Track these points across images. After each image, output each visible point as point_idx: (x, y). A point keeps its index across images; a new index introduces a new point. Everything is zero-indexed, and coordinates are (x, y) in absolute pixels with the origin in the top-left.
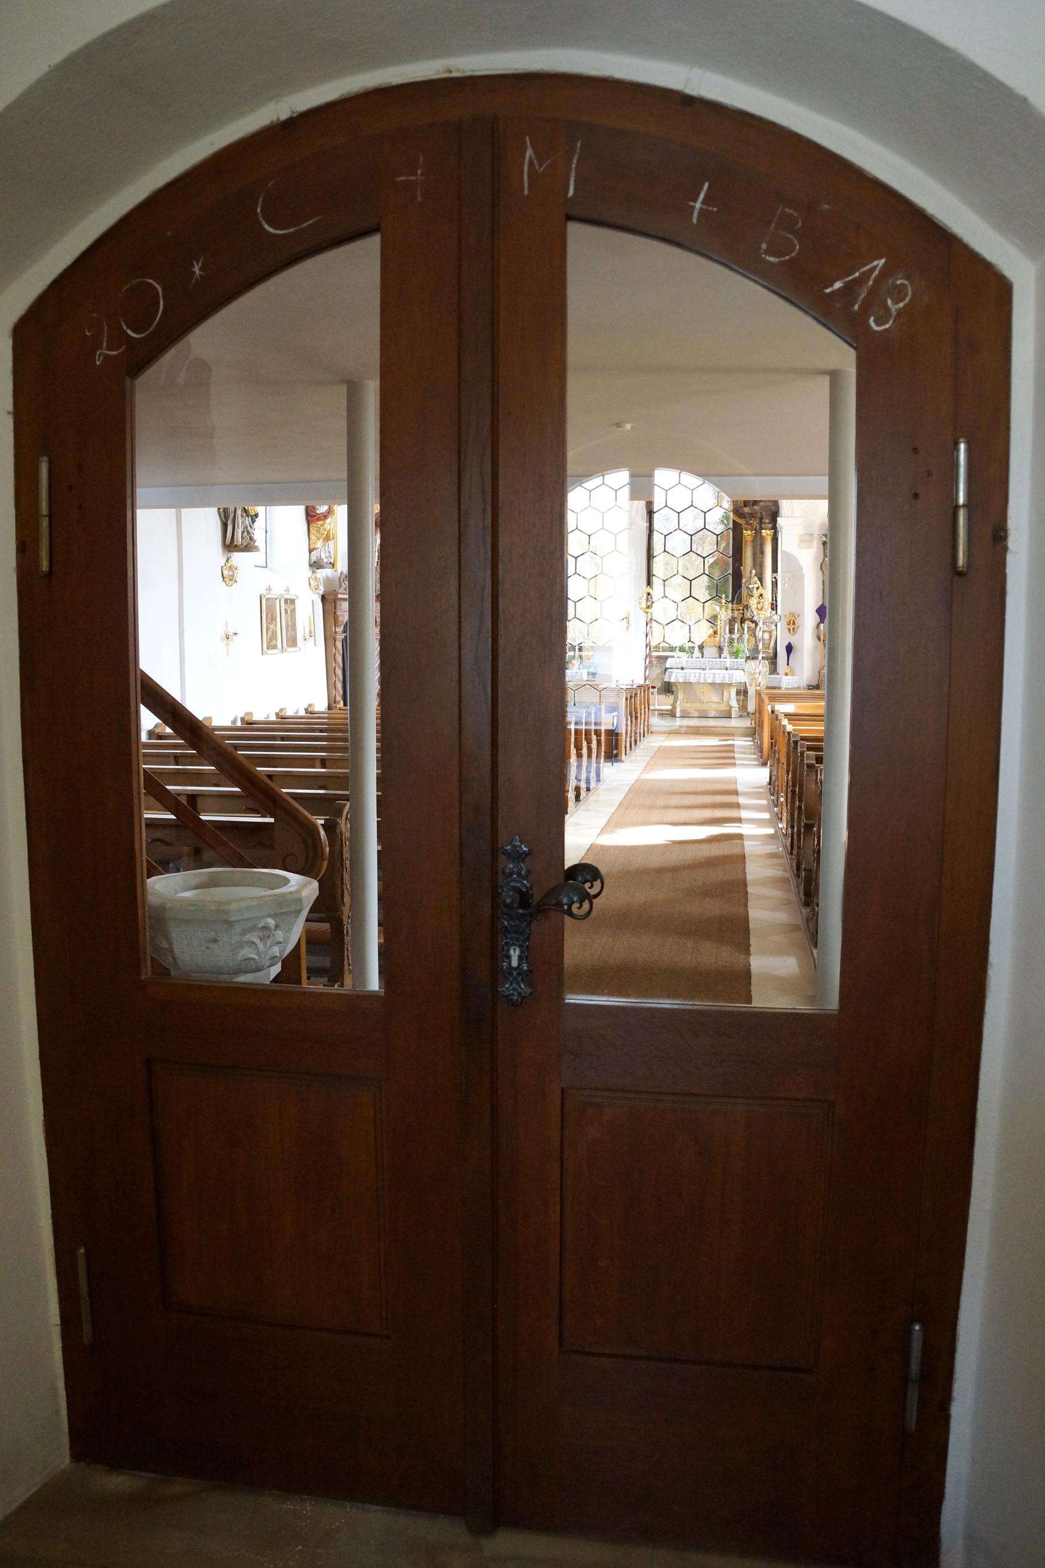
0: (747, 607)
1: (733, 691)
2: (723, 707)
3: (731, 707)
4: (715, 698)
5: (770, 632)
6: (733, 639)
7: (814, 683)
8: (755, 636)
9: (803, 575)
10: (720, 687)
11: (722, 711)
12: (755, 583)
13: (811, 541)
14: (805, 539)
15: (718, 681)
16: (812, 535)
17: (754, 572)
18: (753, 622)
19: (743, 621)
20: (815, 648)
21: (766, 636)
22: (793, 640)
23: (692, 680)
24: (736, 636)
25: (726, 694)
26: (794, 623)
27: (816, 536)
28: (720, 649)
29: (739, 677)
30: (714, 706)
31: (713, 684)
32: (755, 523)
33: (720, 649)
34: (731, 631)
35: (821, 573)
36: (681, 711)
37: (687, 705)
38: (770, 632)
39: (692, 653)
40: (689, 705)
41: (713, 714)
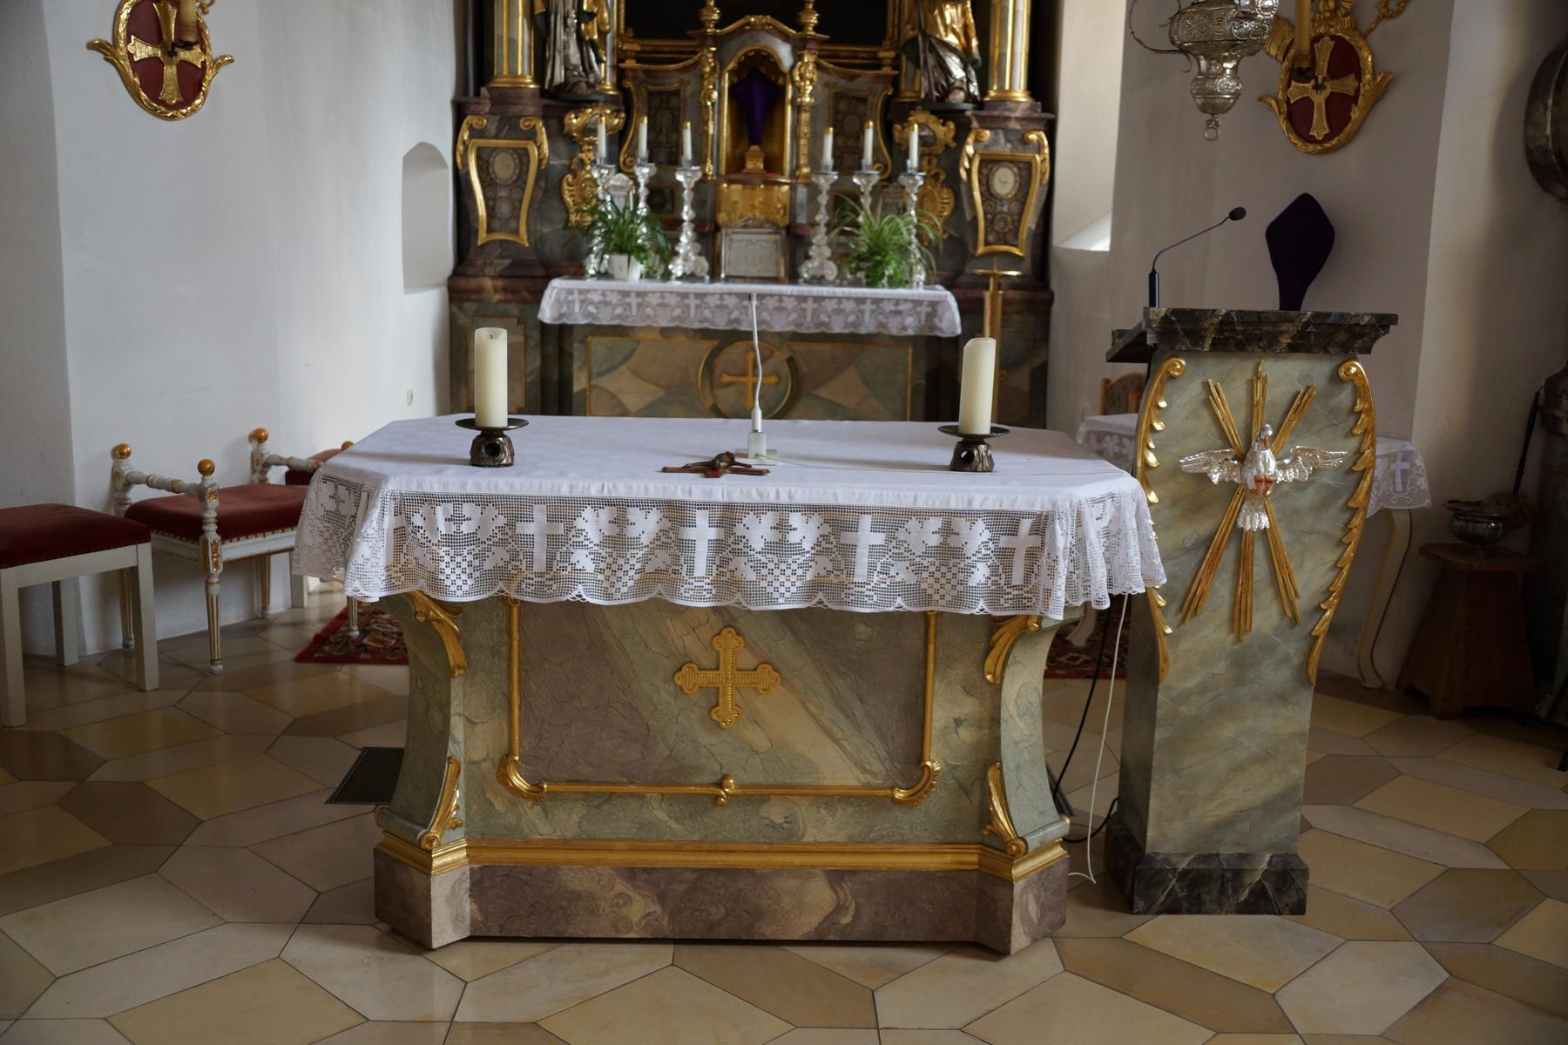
1: (1024, 679)
2: (920, 851)
3: (999, 850)
4: (839, 759)
5: (1025, 171)
6: (855, 195)
10: (882, 657)
11: (903, 886)
15: (877, 585)
18: (945, 112)
19: (893, 117)
21: (1005, 181)
22: (1337, 178)
23: (587, 578)
25: (948, 711)
26: (1345, 61)
28: (794, 242)
30: (822, 827)
31: (822, 629)
33: (794, 242)
34: (848, 158)
36: (482, 882)
37: (539, 824)
38: (1025, 171)
39: (669, 255)
40: (569, 820)
41: (815, 903)
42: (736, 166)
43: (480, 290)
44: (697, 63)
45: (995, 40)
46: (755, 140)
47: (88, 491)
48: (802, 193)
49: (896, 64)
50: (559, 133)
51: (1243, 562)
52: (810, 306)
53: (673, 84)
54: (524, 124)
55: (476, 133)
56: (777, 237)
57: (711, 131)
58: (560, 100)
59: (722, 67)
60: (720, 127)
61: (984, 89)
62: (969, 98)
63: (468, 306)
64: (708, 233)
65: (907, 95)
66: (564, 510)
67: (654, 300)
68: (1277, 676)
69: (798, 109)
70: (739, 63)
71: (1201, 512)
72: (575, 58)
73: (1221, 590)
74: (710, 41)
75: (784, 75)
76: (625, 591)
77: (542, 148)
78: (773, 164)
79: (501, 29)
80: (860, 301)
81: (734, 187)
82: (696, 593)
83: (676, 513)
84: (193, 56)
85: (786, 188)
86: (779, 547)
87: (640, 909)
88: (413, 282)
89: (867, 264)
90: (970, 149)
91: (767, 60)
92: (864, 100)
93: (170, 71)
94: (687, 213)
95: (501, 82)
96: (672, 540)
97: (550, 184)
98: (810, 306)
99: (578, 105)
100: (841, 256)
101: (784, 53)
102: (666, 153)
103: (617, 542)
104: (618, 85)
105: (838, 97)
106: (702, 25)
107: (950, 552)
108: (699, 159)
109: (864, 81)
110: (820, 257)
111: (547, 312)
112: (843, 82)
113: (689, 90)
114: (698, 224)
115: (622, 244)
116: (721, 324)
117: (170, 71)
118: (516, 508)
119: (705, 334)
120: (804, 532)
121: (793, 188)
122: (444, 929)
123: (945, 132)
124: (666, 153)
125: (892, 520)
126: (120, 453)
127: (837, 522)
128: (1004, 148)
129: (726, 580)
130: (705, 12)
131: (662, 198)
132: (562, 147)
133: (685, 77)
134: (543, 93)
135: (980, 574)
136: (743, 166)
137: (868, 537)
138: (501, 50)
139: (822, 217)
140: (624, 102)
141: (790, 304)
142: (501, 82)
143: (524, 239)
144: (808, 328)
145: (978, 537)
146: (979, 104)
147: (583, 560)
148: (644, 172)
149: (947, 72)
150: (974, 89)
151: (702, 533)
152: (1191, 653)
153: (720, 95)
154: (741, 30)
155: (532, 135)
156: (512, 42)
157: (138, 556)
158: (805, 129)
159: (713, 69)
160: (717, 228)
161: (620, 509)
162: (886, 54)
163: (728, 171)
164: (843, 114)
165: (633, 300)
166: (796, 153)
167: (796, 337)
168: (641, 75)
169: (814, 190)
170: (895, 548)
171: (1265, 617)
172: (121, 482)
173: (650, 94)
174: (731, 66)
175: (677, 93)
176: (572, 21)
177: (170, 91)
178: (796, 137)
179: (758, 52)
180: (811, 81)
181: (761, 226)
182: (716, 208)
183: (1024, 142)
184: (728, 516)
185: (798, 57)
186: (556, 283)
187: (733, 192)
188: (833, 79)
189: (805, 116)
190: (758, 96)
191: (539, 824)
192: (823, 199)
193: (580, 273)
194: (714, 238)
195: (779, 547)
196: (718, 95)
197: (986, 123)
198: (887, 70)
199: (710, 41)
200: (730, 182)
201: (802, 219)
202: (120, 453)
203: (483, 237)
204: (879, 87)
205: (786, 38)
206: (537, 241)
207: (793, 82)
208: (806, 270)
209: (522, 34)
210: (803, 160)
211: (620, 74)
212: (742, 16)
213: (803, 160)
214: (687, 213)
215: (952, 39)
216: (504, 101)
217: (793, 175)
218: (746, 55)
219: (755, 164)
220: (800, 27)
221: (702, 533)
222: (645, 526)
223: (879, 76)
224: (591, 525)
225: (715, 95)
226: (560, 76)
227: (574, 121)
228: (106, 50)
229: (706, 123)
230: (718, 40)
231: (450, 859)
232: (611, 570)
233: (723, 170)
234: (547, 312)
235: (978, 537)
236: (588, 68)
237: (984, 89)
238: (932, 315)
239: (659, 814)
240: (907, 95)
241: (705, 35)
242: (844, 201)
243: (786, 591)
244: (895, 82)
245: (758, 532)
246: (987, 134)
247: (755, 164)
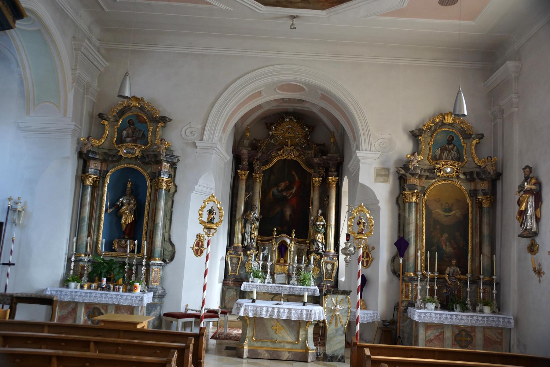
0: (314, 241)
1: (311, 330)
2: (298, 348)
3: (307, 349)
4: (290, 338)
5: (333, 265)
6: (301, 268)
7: (389, 318)
8: (319, 267)
9: (379, 208)
10: (295, 326)
11: (296, 354)
12: (321, 223)
13: (388, 176)
14: (382, 174)
15: (294, 317)
16: (388, 170)
17: (320, 211)
18: (318, 254)
19: (309, 253)
20: (390, 282)
21: (329, 267)
22: (368, 272)
23: (264, 315)
24: (303, 265)
25: (302, 333)
26: (368, 256)
27: (392, 170)
28: (289, 277)
29: (318, 312)
30: (288, 346)
31: (288, 322)
32: (322, 171)
33: (289, 277)
35: (396, 207)
36: (249, 351)
37: (256, 344)
38: (333, 265)
39: (265, 278)
40: (259, 344)
41: (286, 355)
42: (278, 262)
43: (229, 284)
45: (328, 240)
47: (182, 310)
48: (291, 267)
49: (309, 244)
50: (245, 254)
51: (336, 319)
52: (291, 289)
54: (239, 253)
55: (230, 254)
58: (246, 249)
60: (276, 254)
61: (326, 249)
62: (323, 251)
63: (226, 287)
64: (273, 274)
65: (312, 249)
66: (262, 307)
67: (262, 287)
68: (341, 332)
69: (291, 252)
71: (331, 311)
72: (249, 241)
73: (334, 322)
76: (268, 317)
77: (242, 257)
78: (285, 262)
79: (236, 235)
80: (301, 288)
82: (275, 317)
83: (273, 308)
84: (202, 248)
86: (284, 312)
87: (267, 355)
88: (219, 282)
89: (303, 282)
90: (322, 261)
93: (199, 251)
94: (269, 271)
95: (235, 245)
96: (273, 311)
97: (243, 264)
98: (291, 289)
99: (249, 249)
100: (298, 280)
101: (288, 241)
102: (265, 259)
103: (267, 311)
104: (257, 245)
105: (298, 249)
106: (273, 235)
107: (301, 314)
108: (271, 260)
109: (303, 246)
110: (294, 280)
111: (242, 289)
114: (271, 272)
115: (256, 276)
116: (275, 292)
117: (199, 251)
118: (257, 307)
119: (272, 294)
120: (286, 311)
121: (289, 266)
122: (245, 356)
123: (318, 257)
124: (265, 259)
125: (296, 310)
126: (187, 306)
127: (290, 310)
128: (329, 260)
129: (278, 316)
131: (264, 267)
132: (246, 257)
134: (243, 247)
135: (305, 316)
137: (293, 312)
138: (236, 239)
139: (294, 272)
140: (258, 249)
141: (288, 289)
142: (235, 245)
143: (237, 274)
144: (291, 293)
145: (304, 312)
146: (325, 252)
147: (264, 313)
148: (261, 263)
149: (319, 246)
150: (324, 249)
151: (276, 310)
152: (330, 329)
155: (240, 255)
156: (238, 238)
157: (193, 320)
160: (274, 273)
161: (268, 308)
162: (308, 242)
164: (299, 254)
165: (258, 287)
166: (290, 260)
167: (289, 295)
169: (293, 267)
170: (296, 313)
171: (339, 325)
172: (187, 310)
176: (249, 234)
177: (199, 254)
178: (290, 257)
182: (274, 270)
183: (333, 259)
184: (279, 309)
185: (291, 242)
186: (244, 283)
187: (278, 267)
190: (283, 249)
191: (256, 344)
192: (295, 269)
193: (248, 281)
195: (284, 312)
196: (275, 248)
197: (326, 256)
201: (291, 272)
202: (187, 306)
203: (230, 273)
205: (289, 238)
206: (240, 274)
208: (291, 282)
209: (240, 236)
211: (257, 243)
214: (269, 271)
215: (319, 240)
216: (236, 248)
219: (282, 262)
220: (291, 236)
221: (276, 310)
222: (270, 309)
224: (265, 309)
226: (246, 244)
227: (248, 253)
228: (192, 248)
230: (276, 238)
231: (246, 348)
232: (266, 314)
234: (242, 289)
235: (304, 312)
236: (251, 243)
237: (326, 249)
238: (314, 292)
239: (269, 344)
240: (312, 249)
242: (299, 269)
243: (284, 317)
244: (309, 247)
245: (282, 311)
246: (326, 258)
247: (282, 262)
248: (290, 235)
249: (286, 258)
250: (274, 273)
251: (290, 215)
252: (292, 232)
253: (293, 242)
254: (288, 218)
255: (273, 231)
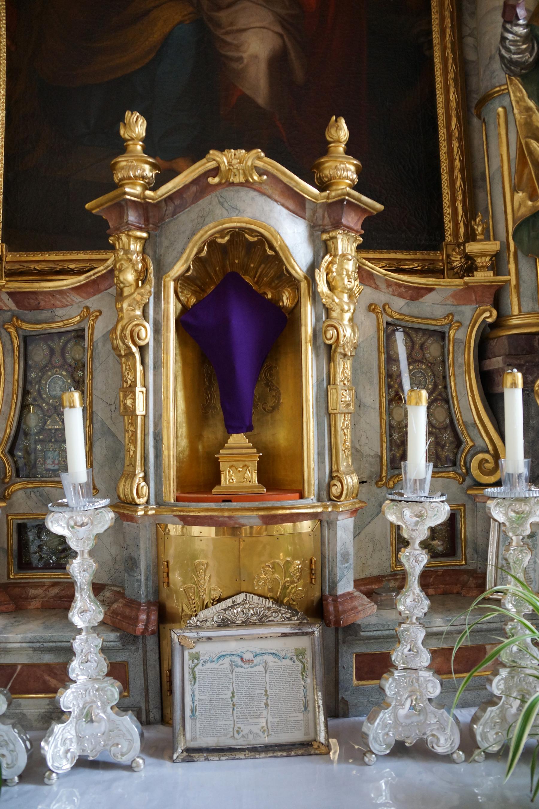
28: (348, 667)
33: (348, 667)
42: (201, 478)
44: (111, 272)
46: (237, 422)
48: (345, 526)
49: (497, 263)
53: (69, 316)
56: (303, 642)
57: (140, 410)
59: (161, 271)
60: (162, 394)
69: (329, 352)
70: (197, 259)
74: (132, 217)
75: (292, 282)
78: (277, 474)
81: (196, 530)
85: (306, 526)
91: (253, 250)
92: (442, 336)
101: (292, 236)
109: (439, 301)
112: (399, 304)
113: (99, 328)
114: (118, 620)
130: (122, 161)
133: (94, 302)
136: (218, 482)
153: (157, 330)
154: (200, 187)
158: (343, 396)
159: (142, 277)
160: (165, 617)
163: (183, 485)
168: (11, 304)
173: (27, 340)
174: (178, 269)
175: (79, 335)
178: (327, 414)
179: (237, 235)
180: (351, 296)
181: (263, 621)
185: (323, 248)
188: (381, 297)
189: (343, 368)
190: (239, 331)
194: (160, 636)
198: (483, 276)
199: (132, 217)
200: (188, 521)
201: (346, 586)
204: (467, 311)
205: (298, 204)
207: (315, 296)
208: (380, 730)
210: (344, 462)
212: (200, 155)
213: (344, 462)
217: (326, 495)
218: (212, 243)
219: (239, 474)
223: (468, 288)
225: (146, 334)
229: (131, 390)
230: (154, 216)
233: (170, 493)
241: (121, 206)
244: (497, 297)
247: (239, 474)
248: (305, 156)
249: (280, 435)
250: (165, 617)
251: (278, 63)
252: (323, 148)
253: (345, 244)
254: (257, 82)
255: (121, 147)
